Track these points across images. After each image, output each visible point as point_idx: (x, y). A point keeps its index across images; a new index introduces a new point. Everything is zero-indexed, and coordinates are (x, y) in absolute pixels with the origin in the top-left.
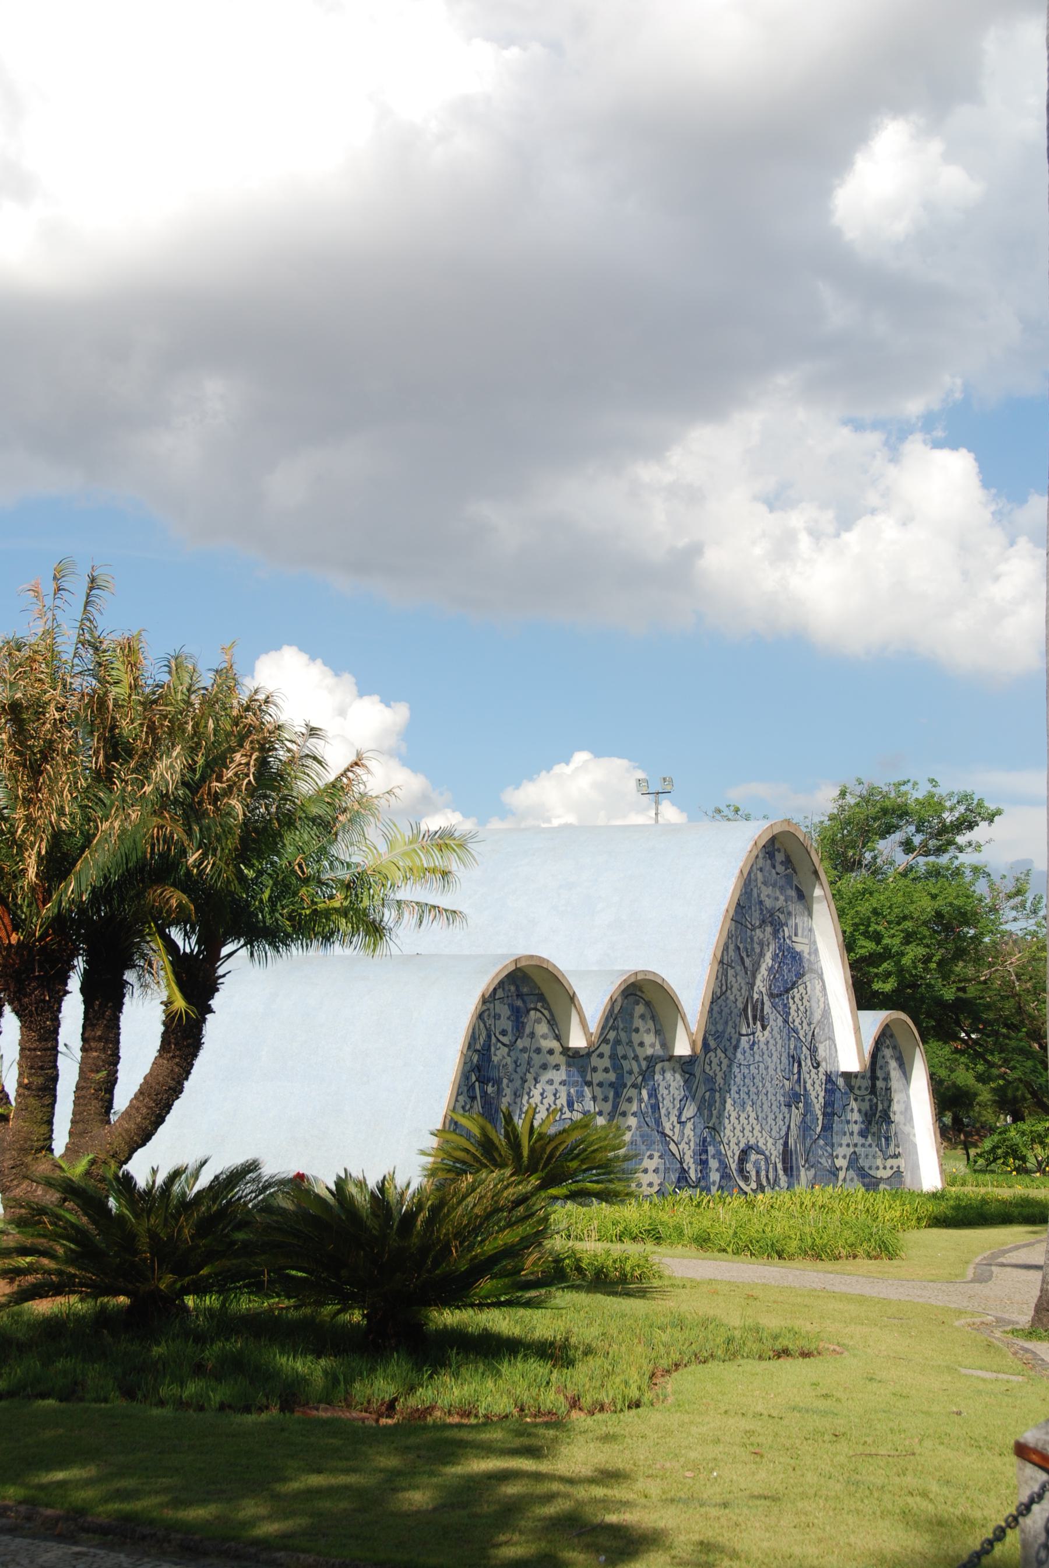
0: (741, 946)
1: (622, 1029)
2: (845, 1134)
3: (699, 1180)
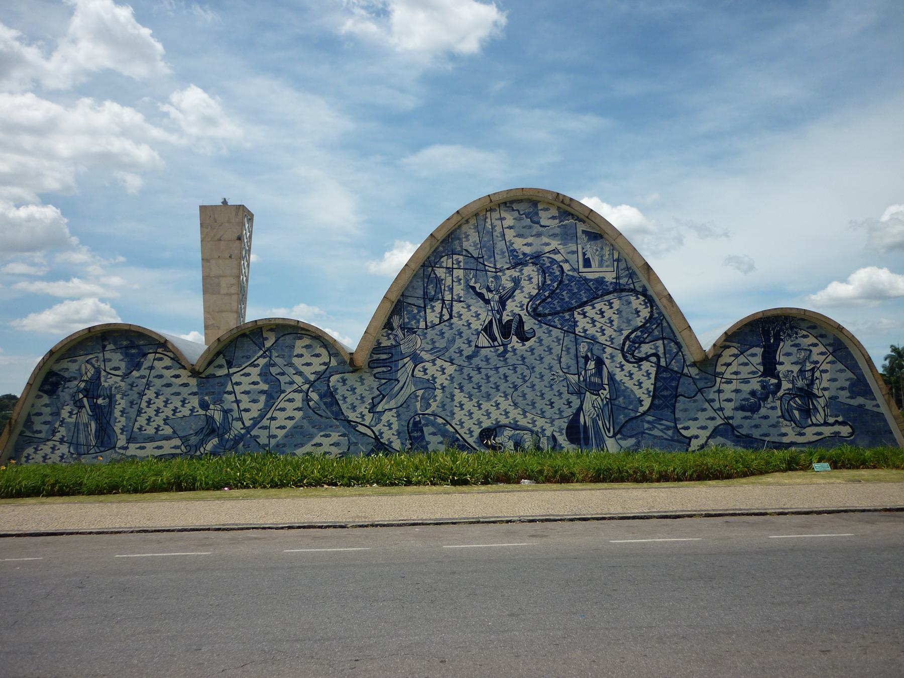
0: (477, 286)
1: (278, 357)
2: (704, 410)
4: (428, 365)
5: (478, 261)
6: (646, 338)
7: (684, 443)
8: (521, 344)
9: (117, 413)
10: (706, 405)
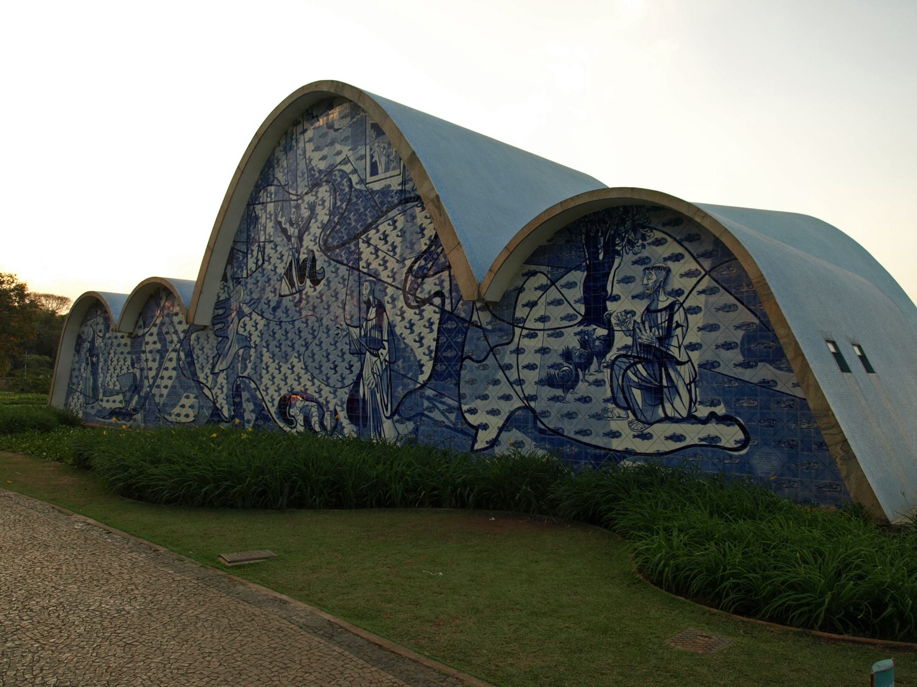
0: (283, 220)
2: (496, 382)
3: (232, 418)
4: (247, 319)
5: (284, 189)
6: (431, 268)
7: (469, 435)
8: (313, 289)
9: (100, 370)
10: (500, 375)
